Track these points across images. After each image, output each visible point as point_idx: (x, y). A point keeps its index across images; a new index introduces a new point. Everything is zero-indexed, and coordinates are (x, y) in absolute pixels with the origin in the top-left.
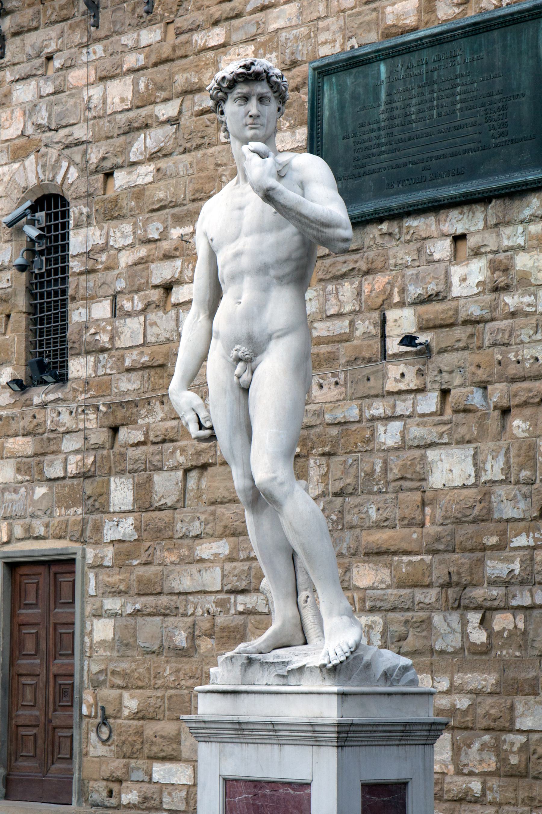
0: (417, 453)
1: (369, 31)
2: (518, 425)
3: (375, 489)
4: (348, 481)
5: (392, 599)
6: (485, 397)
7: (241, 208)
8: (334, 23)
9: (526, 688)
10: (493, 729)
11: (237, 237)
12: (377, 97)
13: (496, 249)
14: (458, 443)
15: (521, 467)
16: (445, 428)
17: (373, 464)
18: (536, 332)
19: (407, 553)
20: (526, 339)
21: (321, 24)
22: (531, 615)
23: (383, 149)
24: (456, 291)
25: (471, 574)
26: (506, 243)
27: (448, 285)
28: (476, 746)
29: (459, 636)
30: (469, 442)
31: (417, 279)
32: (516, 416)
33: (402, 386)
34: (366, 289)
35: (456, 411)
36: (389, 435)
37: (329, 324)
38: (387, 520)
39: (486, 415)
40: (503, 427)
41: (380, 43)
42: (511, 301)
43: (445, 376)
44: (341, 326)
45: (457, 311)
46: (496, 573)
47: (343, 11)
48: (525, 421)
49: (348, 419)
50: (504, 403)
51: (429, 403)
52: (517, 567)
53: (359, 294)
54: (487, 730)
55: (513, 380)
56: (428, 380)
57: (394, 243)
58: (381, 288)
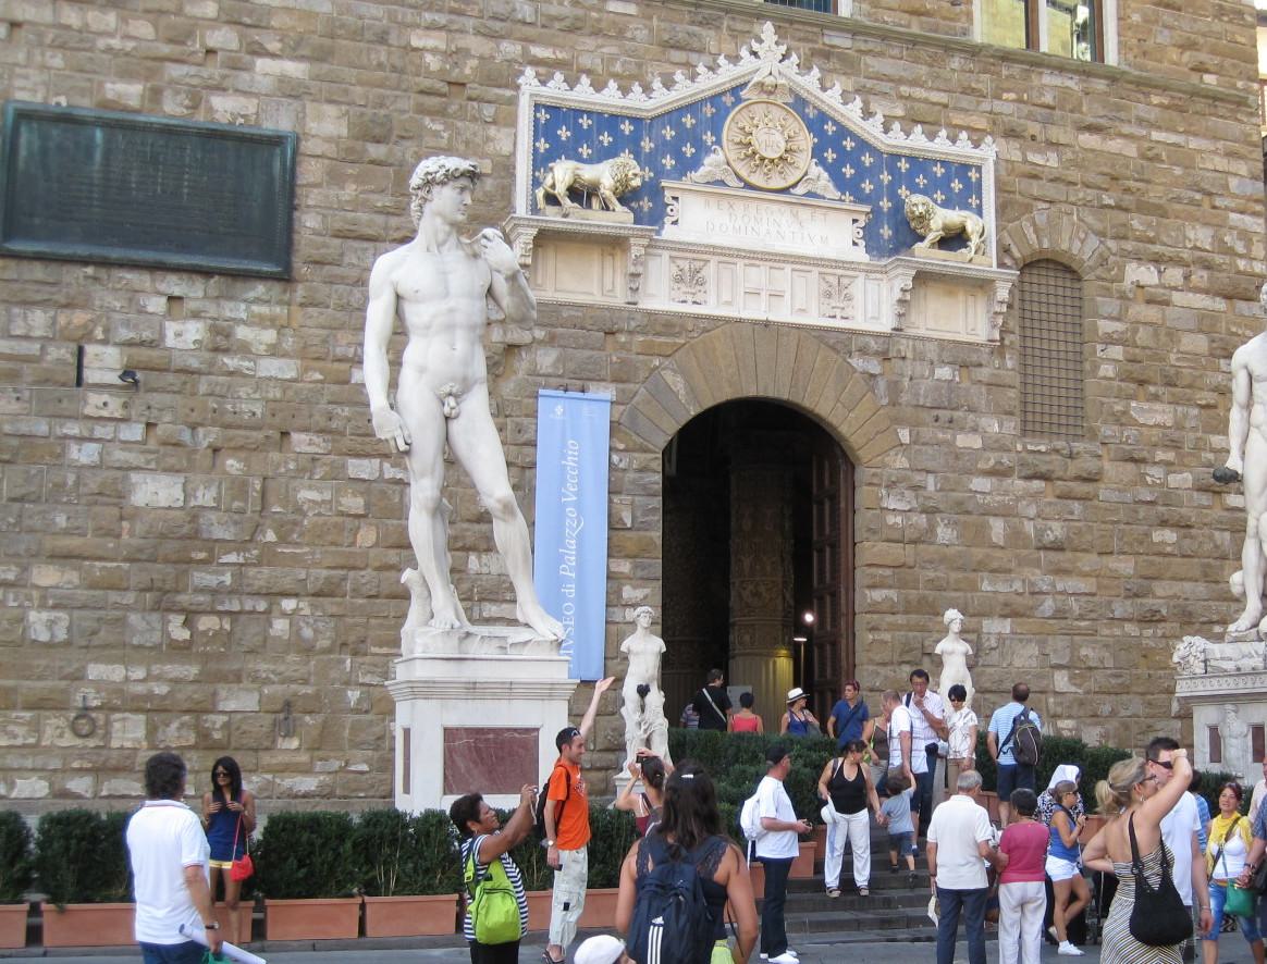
0: (119, 474)
1: (83, 96)
2: (233, 465)
3: (65, 499)
4: (33, 489)
5: (83, 598)
6: (193, 436)
7: (444, 273)
8: (36, 76)
9: (231, 677)
10: (195, 711)
11: (446, 295)
12: (89, 155)
13: (216, 316)
14: (166, 470)
15: (233, 499)
16: (152, 456)
17: (65, 477)
18: (255, 392)
19: (101, 559)
20: (244, 396)
21: (18, 70)
22: (237, 620)
23: (95, 203)
24: (170, 341)
25: (177, 582)
26: (228, 314)
27: (162, 336)
28: (175, 725)
29: (159, 634)
30: (178, 471)
31: (127, 324)
32: (230, 457)
33: (105, 413)
34: (62, 320)
35: (165, 444)
36: (84, 454)
37: (13, 343)
38: (78, 528)
39: (195, 451)
40: (214, 465)
41: (91, 110)
42: (231, 362)
43: (155, 413)
44: (35, 348)
45: (170, 362)
46: (205, 583)
47: (49, 68)
48: (239, 461)
49: (34, 433)
50: (219, 445)
51: (135, 432)
52: (228, 579)
53: (54, 321)
54: (187, 711)
55: (229, 426)
56: (133, 413)
57: (98, 287)
58: (82, 322)
